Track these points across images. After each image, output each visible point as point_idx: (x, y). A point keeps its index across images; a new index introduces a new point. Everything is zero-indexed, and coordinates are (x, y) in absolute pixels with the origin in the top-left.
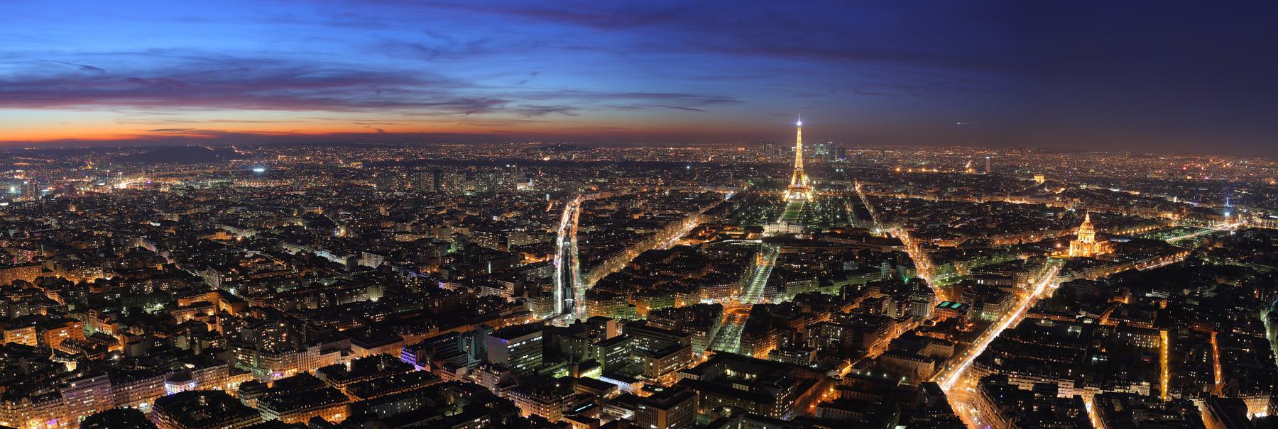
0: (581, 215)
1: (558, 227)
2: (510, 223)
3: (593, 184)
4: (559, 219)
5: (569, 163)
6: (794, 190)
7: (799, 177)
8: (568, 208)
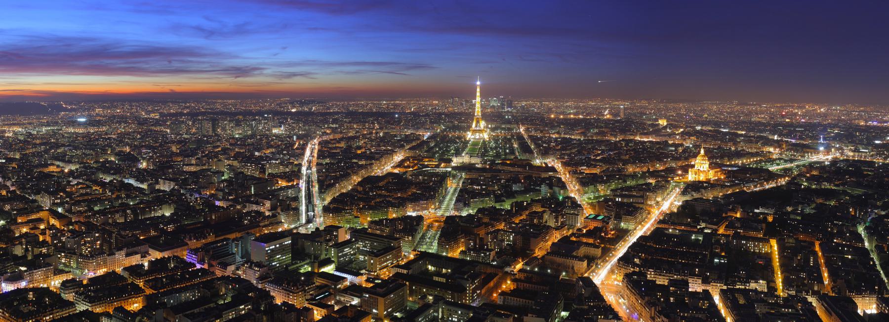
0: (319, 151)
1: (303, 160)
2: (267, 157)
3: (328, 128)
4: (303, 154)
5: (310, 113)
6: (475, 131)
7: (478, 122)
8: (309, 146)
